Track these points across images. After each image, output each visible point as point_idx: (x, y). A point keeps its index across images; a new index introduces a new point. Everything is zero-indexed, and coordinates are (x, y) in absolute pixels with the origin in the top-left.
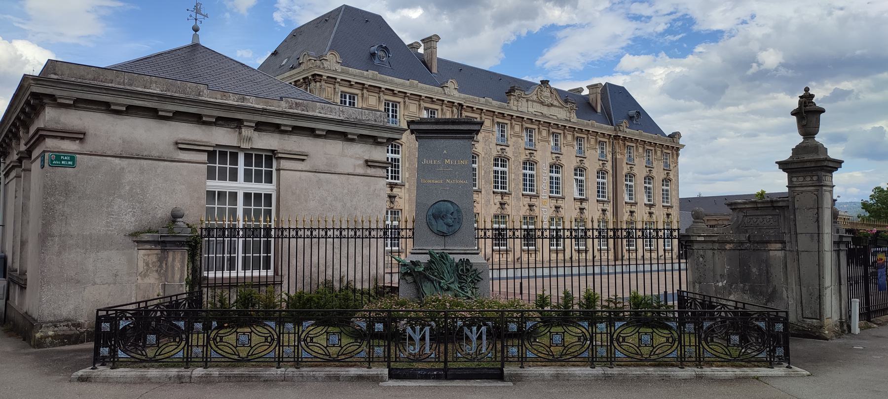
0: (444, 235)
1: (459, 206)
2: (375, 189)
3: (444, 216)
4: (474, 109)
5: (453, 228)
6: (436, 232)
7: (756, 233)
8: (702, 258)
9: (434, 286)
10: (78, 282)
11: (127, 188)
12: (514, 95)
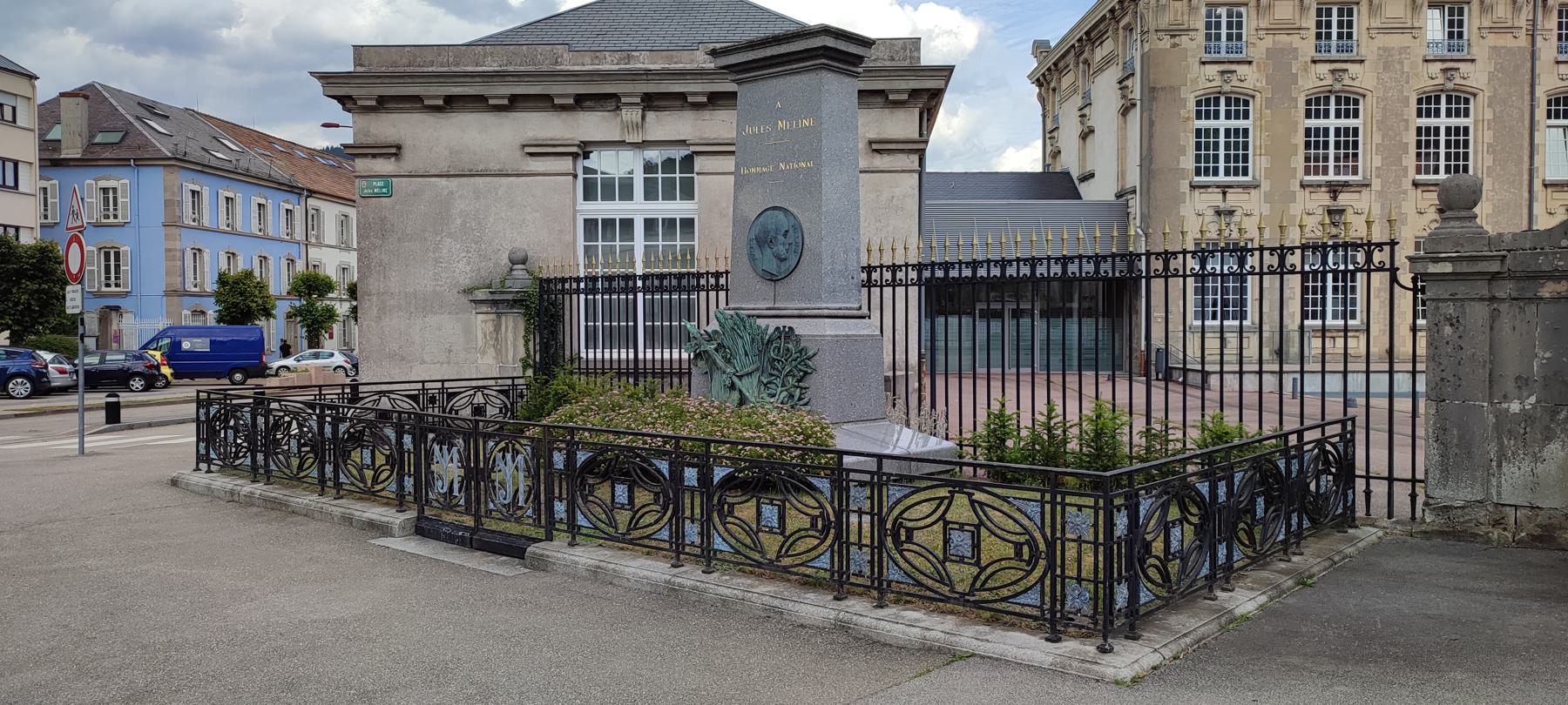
0: (773, 279)
2: (893, 197)
8: (1452, 325)
10: (403, 359)
11: (459, 221)
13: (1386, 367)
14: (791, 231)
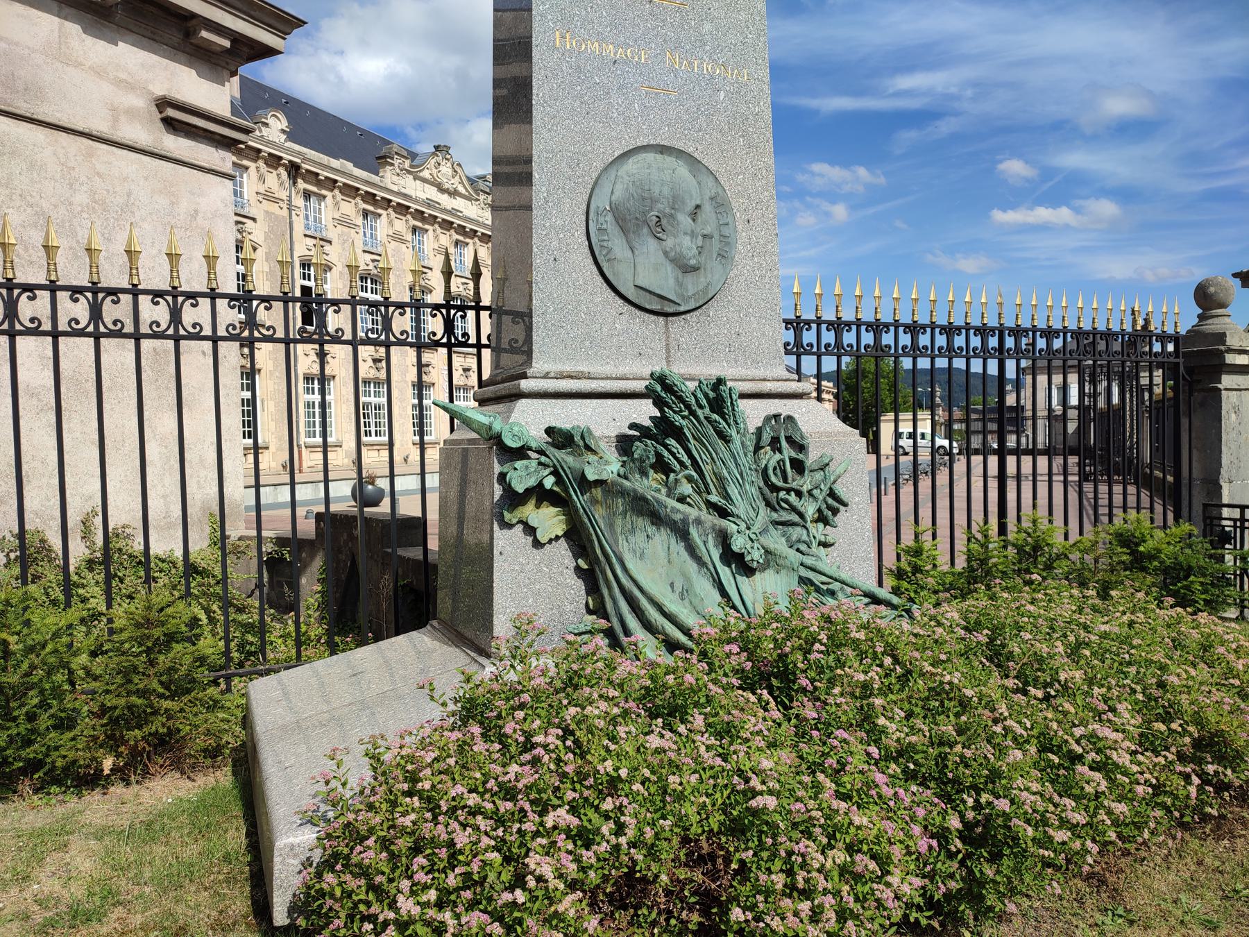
1: (721, 180)
3: (664, 222)
4: (321, 177)
6: (631, 293)
9: (692, 550)
12: (392, 165)
13: (287, 479)
14: (708, 208)
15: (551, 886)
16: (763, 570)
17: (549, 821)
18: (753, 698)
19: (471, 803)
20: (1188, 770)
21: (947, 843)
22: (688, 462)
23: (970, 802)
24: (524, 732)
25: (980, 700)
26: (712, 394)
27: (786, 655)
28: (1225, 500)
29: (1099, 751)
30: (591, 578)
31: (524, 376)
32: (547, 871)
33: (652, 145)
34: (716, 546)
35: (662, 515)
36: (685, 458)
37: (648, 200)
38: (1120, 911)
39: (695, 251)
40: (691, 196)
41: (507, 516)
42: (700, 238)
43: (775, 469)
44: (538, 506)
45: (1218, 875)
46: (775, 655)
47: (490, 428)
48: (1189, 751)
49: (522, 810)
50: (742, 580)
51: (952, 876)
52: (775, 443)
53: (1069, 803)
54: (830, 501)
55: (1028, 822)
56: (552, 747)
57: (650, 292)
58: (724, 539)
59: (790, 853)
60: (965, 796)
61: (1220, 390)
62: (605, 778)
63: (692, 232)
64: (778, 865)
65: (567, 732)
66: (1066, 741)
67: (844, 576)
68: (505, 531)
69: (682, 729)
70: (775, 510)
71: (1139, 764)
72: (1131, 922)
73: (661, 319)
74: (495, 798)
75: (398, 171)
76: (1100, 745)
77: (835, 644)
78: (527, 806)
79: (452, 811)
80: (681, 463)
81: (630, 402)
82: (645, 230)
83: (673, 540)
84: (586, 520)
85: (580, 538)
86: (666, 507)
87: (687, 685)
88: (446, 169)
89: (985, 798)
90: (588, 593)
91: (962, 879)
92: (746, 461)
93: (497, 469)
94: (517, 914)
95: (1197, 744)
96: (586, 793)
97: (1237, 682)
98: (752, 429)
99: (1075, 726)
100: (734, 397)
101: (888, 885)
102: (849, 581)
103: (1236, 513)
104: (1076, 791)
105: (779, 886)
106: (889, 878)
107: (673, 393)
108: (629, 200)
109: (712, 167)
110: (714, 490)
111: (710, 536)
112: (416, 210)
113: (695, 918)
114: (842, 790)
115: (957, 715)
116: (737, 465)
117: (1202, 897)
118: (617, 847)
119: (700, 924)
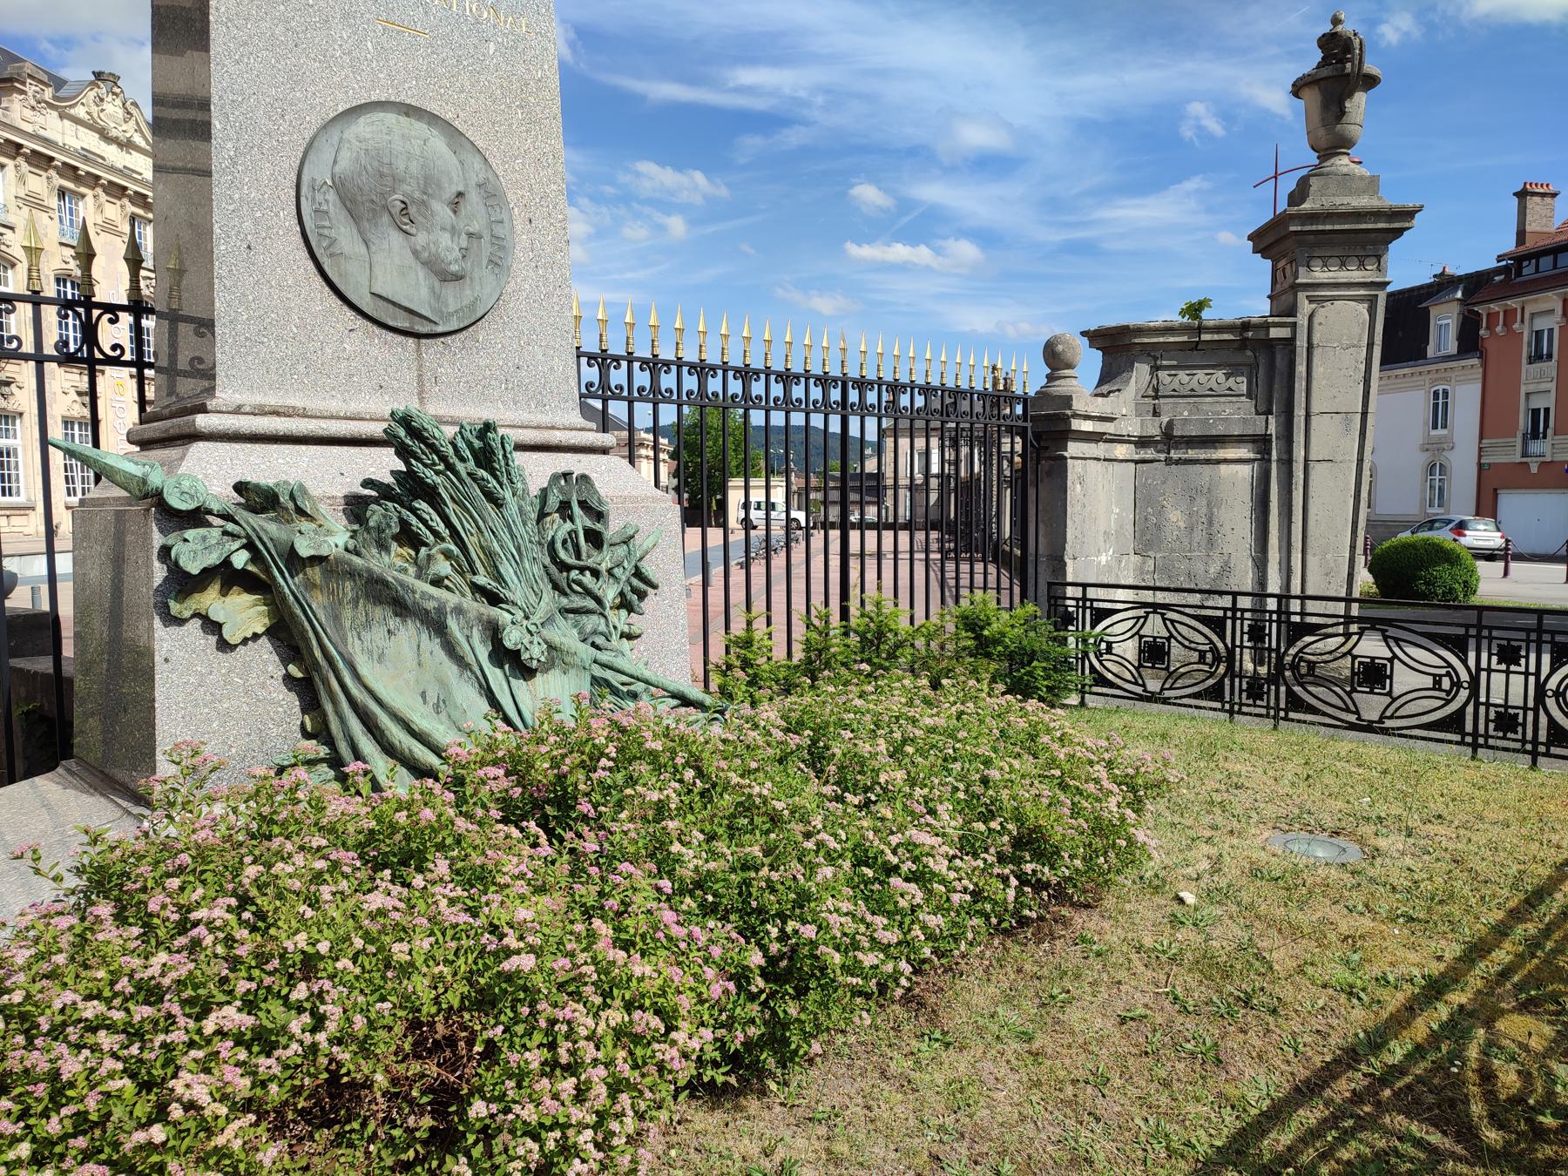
3: (412, 210)
5: (468, 294)
6: (366, 304)
7: (1186, 413)
9: (450, 648)
12: (23, 92)
14: (474, 197)
15: (207, 1113)
16: (546, 671)
17: (209, 1026)
18: (516, 833)
19: (89, 1014)
20: (1007, 871)
21: (749, 984)
22: (445, 533)
23: (774, 932)
24: (180, 907)
25: (792, 813)
26: (477, 444)
27: (565, 776)
28: (1070, 579)
29: (915, 860)
30: (308, 691)
31: (203, 409)
32: (201, 1094)
33: (393, 103)
34: (483, 642)
35: (409, 602)
36: (441, 527)
37: (387, 177)
38: (937, 1035)
39: (457, 254)
40: (451, 179)
41: (175, 607)
42: (464, 236)
43: (564, 542)
44: (224, 592)
45: (1036, 982)
46: (551, 778)
47: (144, 482)
48: (1008, 849)
49: (170, 1016)
50: (519, 685)
51: (752, 1021)
52: (565, 509)
53: (880, 921)
54: (635, 582)
55: (837, 949)
56: (218, 923)
57: (394, 304)
58: (494, 632)
59: (553, 1022)
60: (769, 927)
61: (1066, 458)
62: (298, 958)
63: (453, 227)
64: (538, 1037)
65: (245, 901)
66: (882, 852)
67: (647, 674)
68: (173, 630)
69: (418, 881)
70: (565, 594)
71: (957, 870)
72: (947, 1045)
73: (411, 341)
74: (130, 1005)
75: (33, 103)
76: (917, 852)
77: (625, 758)
78: (176, 1009)
79: (57, 1032)
80: (436, 534)
81: (366, 450)
82: (386, 219)
83: (425, 636)
84: (298, 611)
85: (291, 636)
86: (414, 592)
87: (423, 823)
88: (113, 108)
89: (791, 925)
90: (304, 711)
91: (765, 1023)
92: (526, 532)
93: (158, 540)
94: (155, 1158)
95: (1018, 843)
96: (268, 980)
97: (1057, 773)
98: (534, 490)
99: (892, 833)
100: (508, 448)
101: (674, 1043)
102: (653, 679)
103: (1078, 592)
104: (890, 907)
105: (535, 1065)
106: (673, 1035)
107: (423, 440)
108: (360, 175)
109: (480, 144)
110: (481, 570)
111: (475, 629)
112: (64, 164)
113: (427, 1121)
114: (623, 936)
115: (768, 832)
116: (513, 536)
117: (1018, 1007)
118: (314, 1048)
119: (432, 1129)
